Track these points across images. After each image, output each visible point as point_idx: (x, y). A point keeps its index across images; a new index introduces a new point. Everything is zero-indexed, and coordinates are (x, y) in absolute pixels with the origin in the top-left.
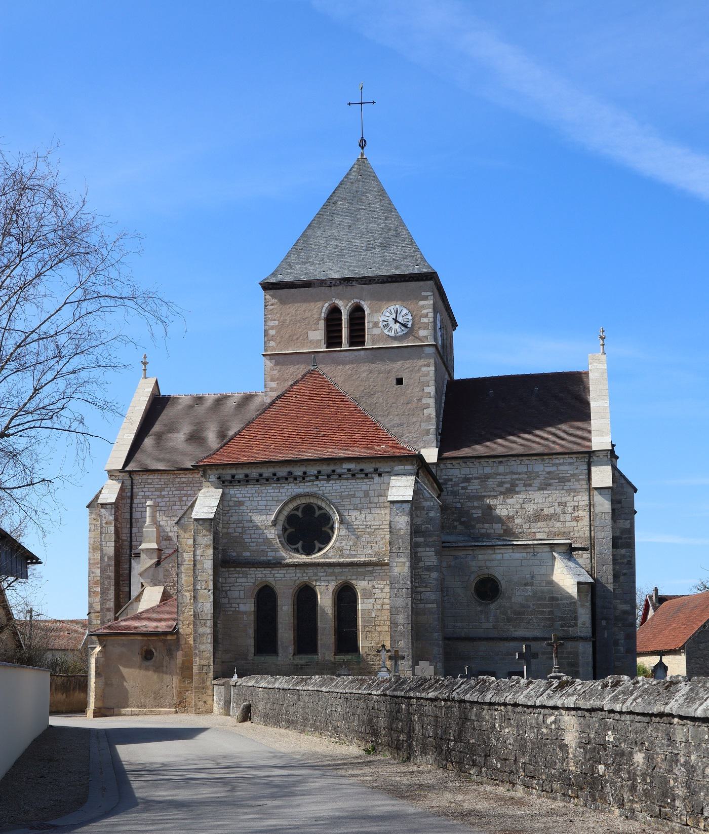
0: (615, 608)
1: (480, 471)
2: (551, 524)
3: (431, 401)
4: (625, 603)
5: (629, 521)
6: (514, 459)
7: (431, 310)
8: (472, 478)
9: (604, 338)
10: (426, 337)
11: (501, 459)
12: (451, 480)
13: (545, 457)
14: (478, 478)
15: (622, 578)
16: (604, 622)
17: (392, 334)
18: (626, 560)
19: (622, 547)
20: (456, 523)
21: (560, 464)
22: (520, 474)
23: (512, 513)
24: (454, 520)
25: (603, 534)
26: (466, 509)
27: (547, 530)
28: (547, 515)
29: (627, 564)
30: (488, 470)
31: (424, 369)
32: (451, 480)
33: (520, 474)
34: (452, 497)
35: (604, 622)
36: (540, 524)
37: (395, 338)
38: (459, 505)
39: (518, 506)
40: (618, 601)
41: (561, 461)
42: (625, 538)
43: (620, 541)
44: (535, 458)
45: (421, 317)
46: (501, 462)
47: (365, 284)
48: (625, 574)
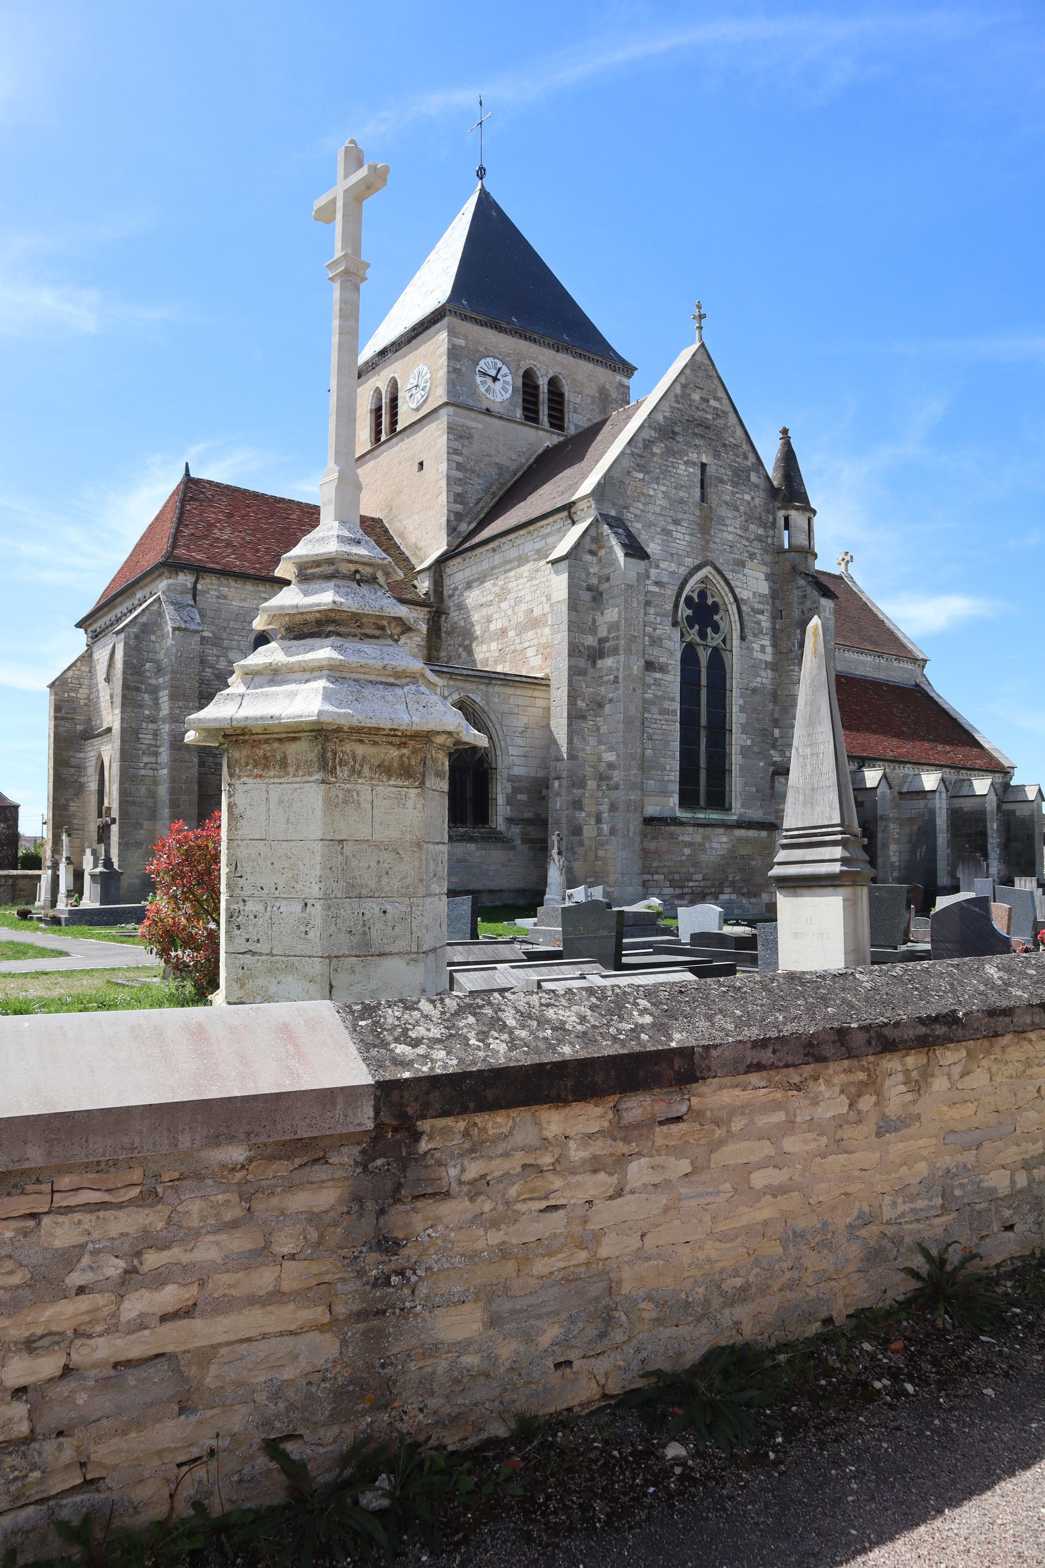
0: (600, 760)
1: (480, 569)
2: (539, 631)
3: (444, 483)
4: (611, 749)
5: (617, 609)
6: (503, 540)
7: (445, 357)
8: (472, 582)
9: (701, 317)
10: (440, 396)
11: (492, 545)
12: (456, 589)
13: (531, 528)
14: (479, 579)
15: (608, 708)
16: (556, 783)
17: (414, 406)
18: (612, 677)
19: (609, 656)
20: (461, 650)
21: (548, 535)
22: (511, 561)
23: (506, 624)
24: (460, 646)
25: (559, 636)
26: (468, 627)
27: (535, 641)
28: (536, 619)
29: (614, 682)
30: (485, 565)
31: (439, 440)
32: (456, 589)
33: (511, 561)
34: (457, 613)
35: (556, 783)
36: (531, 634)
37: (417, 409)
38: (462, 623)
39: (510, 612)
40: (603, 747)
41: (549, 529)
42: (613, 638)
43: (607, 645)
44: (522, 532)
45: (438, 370)
46: (494, 550)
47: (397, 351)
48: (611, 700)
